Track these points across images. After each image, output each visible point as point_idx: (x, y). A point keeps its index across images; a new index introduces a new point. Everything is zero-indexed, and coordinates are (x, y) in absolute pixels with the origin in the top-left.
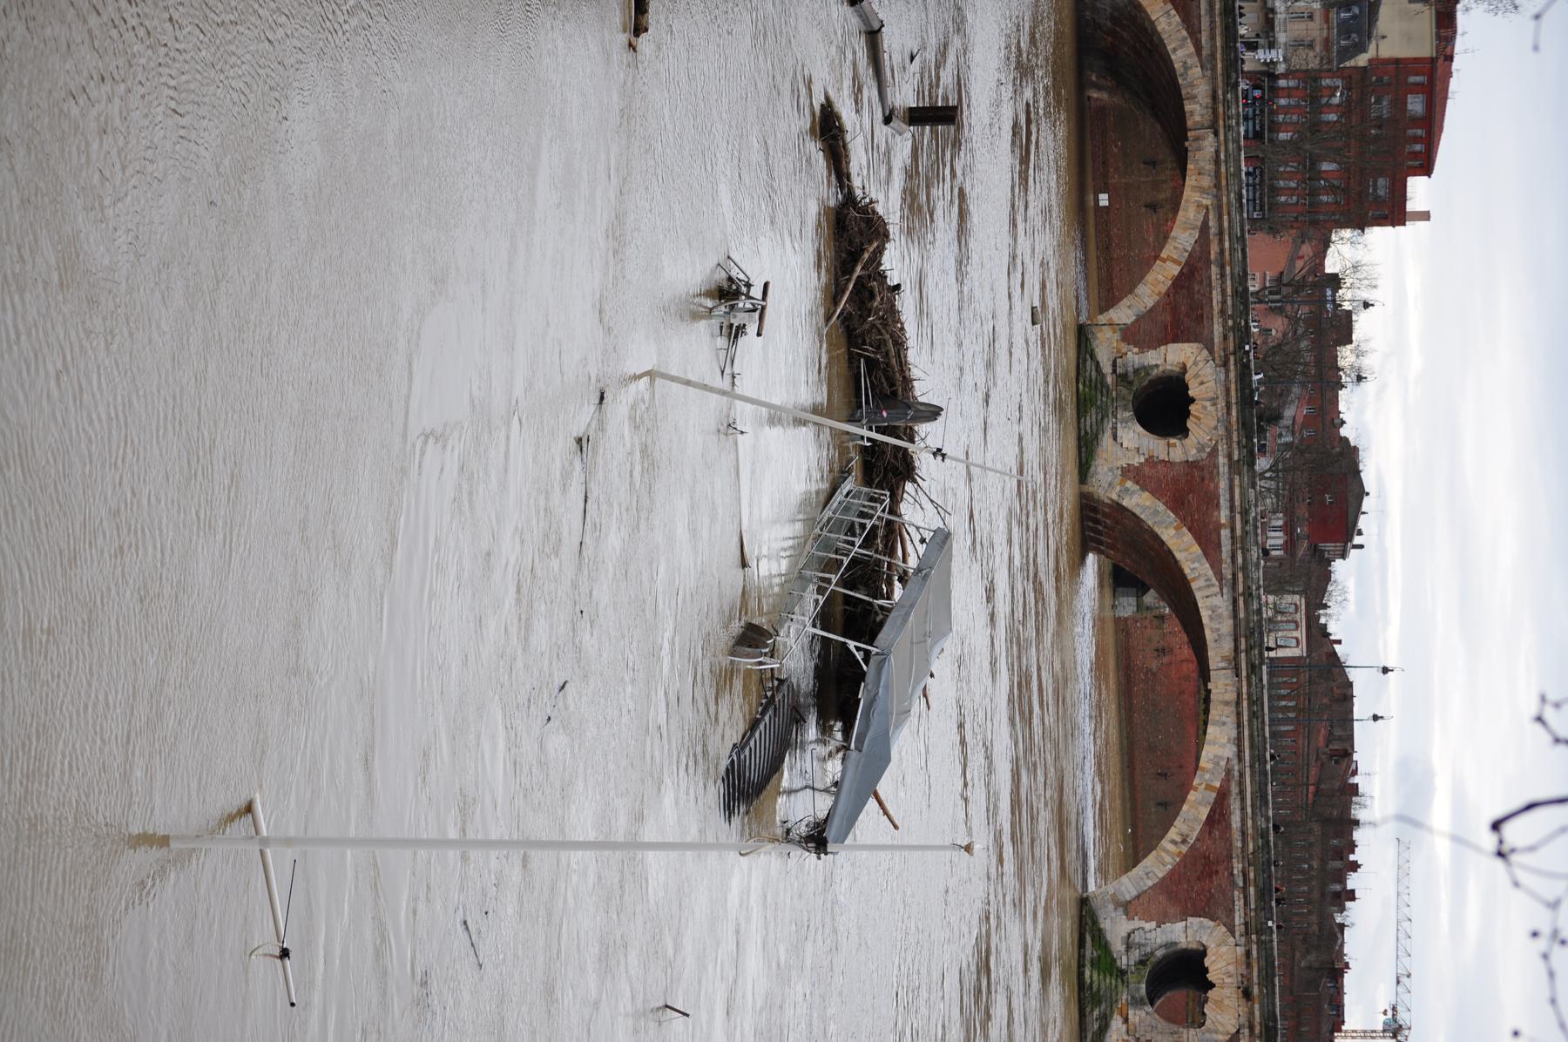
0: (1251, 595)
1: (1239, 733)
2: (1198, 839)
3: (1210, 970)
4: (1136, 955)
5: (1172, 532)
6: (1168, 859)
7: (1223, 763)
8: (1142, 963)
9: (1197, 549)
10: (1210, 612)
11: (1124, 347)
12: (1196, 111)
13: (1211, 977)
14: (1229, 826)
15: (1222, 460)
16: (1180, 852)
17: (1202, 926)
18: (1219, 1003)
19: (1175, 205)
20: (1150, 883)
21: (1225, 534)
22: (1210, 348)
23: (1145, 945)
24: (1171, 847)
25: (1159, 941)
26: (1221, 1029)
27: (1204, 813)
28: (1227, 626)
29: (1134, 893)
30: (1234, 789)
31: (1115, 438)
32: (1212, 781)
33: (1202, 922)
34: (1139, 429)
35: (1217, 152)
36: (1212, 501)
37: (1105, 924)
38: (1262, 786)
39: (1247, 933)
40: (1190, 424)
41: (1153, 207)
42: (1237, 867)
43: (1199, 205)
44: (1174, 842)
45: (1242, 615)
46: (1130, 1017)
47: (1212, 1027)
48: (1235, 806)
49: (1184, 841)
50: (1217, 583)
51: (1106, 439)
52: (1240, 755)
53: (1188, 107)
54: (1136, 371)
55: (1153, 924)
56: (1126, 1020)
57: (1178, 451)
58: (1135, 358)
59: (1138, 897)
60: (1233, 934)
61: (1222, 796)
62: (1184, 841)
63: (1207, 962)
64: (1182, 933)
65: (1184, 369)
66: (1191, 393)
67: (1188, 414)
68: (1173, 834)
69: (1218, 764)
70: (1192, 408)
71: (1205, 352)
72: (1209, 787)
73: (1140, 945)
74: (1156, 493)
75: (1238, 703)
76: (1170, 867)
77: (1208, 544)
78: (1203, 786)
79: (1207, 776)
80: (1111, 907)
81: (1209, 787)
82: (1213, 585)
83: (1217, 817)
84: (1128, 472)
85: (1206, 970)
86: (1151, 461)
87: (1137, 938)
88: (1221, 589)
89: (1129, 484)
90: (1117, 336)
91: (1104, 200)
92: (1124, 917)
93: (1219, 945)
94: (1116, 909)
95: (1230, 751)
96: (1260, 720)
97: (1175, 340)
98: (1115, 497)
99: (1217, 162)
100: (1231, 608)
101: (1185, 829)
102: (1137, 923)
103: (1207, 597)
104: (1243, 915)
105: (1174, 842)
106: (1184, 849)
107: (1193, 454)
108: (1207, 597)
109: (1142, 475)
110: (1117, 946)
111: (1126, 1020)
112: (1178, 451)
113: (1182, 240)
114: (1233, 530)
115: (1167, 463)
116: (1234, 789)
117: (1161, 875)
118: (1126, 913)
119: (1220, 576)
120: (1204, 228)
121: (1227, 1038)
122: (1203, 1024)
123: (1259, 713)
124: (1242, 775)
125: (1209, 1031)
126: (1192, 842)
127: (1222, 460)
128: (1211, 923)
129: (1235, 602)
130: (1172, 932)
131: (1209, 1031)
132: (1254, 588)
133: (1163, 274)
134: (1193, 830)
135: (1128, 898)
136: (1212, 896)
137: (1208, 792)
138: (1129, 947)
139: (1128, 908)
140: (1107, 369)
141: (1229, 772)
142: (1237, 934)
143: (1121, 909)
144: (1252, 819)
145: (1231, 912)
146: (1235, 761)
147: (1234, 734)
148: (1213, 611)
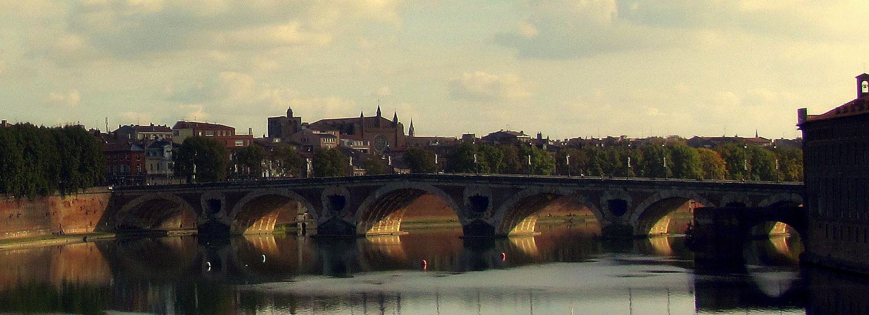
15: (226, 191)
42: (311, 187)
56: (344, 217)
57: (223, 202)
61: (295, 191)
66: (211, 199)
75: (276, 187)
139: (320, 215)
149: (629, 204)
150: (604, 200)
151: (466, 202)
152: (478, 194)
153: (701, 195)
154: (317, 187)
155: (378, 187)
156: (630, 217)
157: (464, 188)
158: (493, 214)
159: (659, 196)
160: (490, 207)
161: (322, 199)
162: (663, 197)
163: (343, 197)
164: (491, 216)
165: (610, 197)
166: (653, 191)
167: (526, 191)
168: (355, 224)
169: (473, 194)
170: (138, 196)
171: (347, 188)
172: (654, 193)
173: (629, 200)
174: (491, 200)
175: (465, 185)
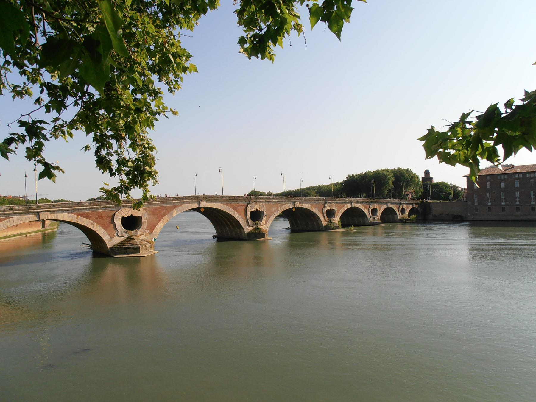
0: (12, 209)
1: (60, 211)
2: (92, 220)
3: (128, 215)
4: (125, 234)
6: (98, 228)
7: (69, 215)
8: (126, 233)
10: (19, 221)
16: (96, 225)
17: (116, 218)
18: (136, 213)
20: (105, 232)
23: (122, 232)
24: (95, 227)
25: (121, 229)
26: (142, 212)
27: (84, 219)
28: (24, 217)
29: (108, 235)
32: (75, 218)
33: (116, 218)
37: (117, 242)
38: (76, 204)
44: (93, 227)
45: (21, 211)
46: (140, 234)
47: (142, 214)
49: (93, 224)
50: (8, 219)
59: (109, 235)
61: (79, 215)
62: (93, 224)
69: (70, 216)
73: (122, 233)
76: (100, 227)
78: (77, 220)
79: (74, 219)
81: (77, 218)
82: (9, 220)
85: (128, 216)
88: (10, 218)
92: (114, 238)
94: (112, 240)
95: (66, 214)
96: (56, 205)
100: (17, 215)
101: (90, 224)
103: (14, 222)
104: (113, 208)
105: (93, 227)
106: (95, 224)
108: (14, 222)
110: (122, 239)
111: (141, 235)
117: (103, 229)
118: (114, 237)
121: (144, 211)
122: (141, 217)
123: (54, 205)
124: (73, 210)
125: (143, 215)
126: (93, 222)
128: (116, 216)
129: (15, 214)
130: (118, 226)
131: (143, 215)
132: (10, 208)
134: (89, 222)
135: (109, 237)
136: (108, 216)
137: (78, 218)
139: (112, 238)
142: (118, 209)
143: (112, 239)
144: (87, 206)
146: (69, 211)
148: (19, 220)
149: (336, 212)
152: (257, 209)
155: (175, 207)
158: (266, 222)
160: (264, 219)
162: (349, 207)
163: (140, 218)
165: (328, 208)
167: (285, 206)
168: (154, 241)
169: (253, 210)
173: (336, 210)
174: (265, 213)
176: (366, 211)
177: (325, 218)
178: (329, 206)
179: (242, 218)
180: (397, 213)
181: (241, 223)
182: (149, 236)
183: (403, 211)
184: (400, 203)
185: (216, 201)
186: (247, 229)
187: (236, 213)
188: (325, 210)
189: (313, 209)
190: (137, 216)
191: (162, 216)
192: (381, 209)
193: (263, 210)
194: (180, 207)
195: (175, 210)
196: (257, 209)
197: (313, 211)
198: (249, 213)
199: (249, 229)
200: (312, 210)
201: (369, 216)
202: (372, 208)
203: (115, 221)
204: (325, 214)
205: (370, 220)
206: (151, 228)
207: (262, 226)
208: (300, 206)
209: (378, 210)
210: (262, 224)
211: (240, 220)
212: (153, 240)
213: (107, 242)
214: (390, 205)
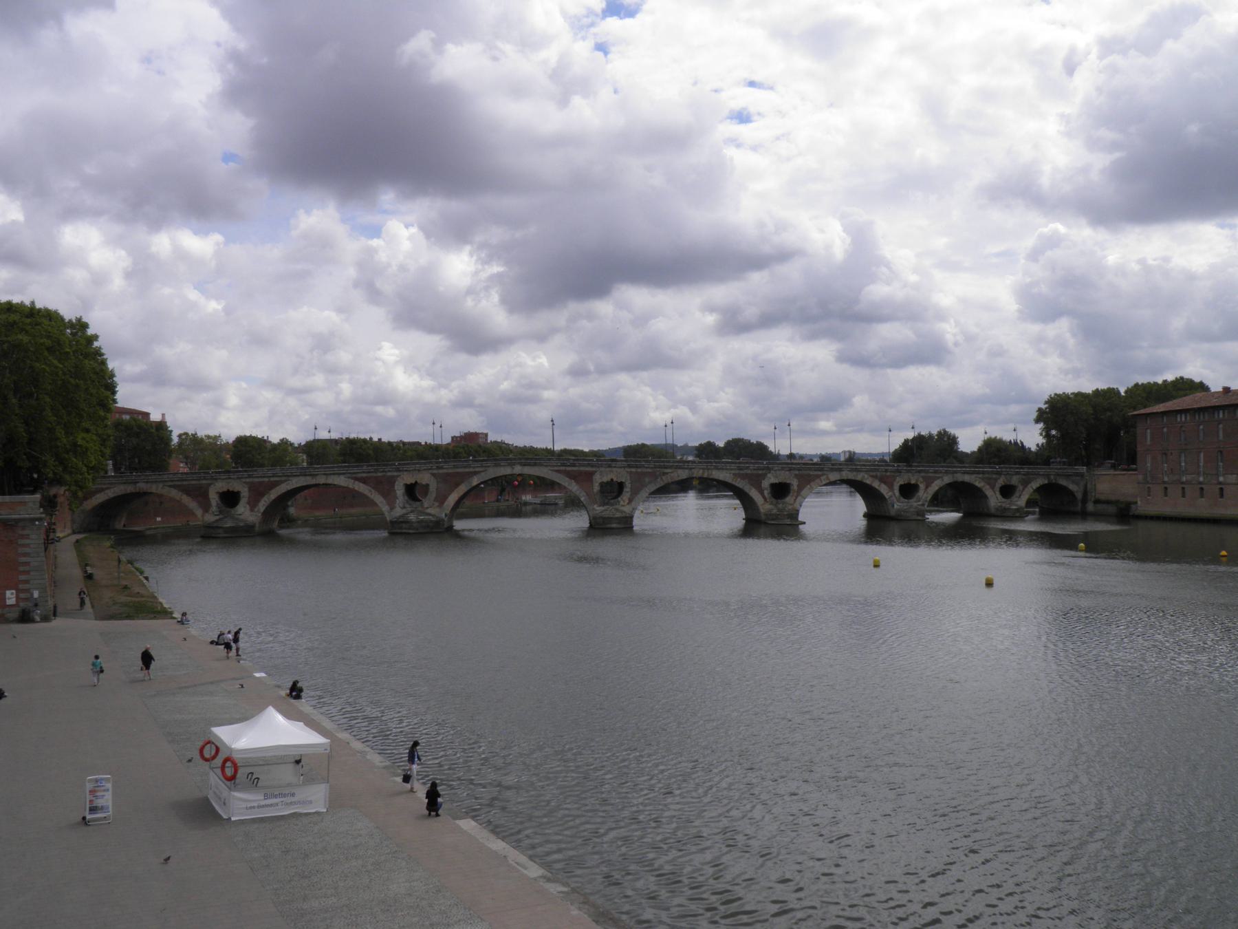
2: (370, 486)
4: (407, 506)
5: (271, 496)
7: (347, 479)
9: (278, 488)
11: (210, 512)
12: (130, 489)
13: (413, 482)
14: (366, 477)
15: (248, 480)
19: (160, 496)
21: (272, 479)
22: (210, 485)
27: (361, 484)
28: (302, 478)
30: (354, 475)
31: (240, 515)
34: (238, 506)
35: (144, 482)
36: (261, 483)
37: (398, 515)
39: (400, 471)
40: (236, 490)
41: (161, 503)
43: (162, 488)
48: (360, 475)
49: (371, 491)
51: (241, 517)
52: (344, 474)
53: (129, 492)
54: (219, 508)
55: (397, 500)
56: (427, 508)
57: (245, 493)
58: (214, 508)
60: (400, 475)
61: (356, 479)
63: (408, 483)
64: (400, 491)
65: (218, 493)
67: (233, 492)
68: (369, 495)
70: (231, 490)
71: (212, 486)
72: (354, 483)
74: (258, 501)
77: (274, 485)
80: (392, 513)
81: (354, 483)
83: (364, 481)
84: (252, 510)
86: (249, 503)
87: (401, 505)
89: (256, 510)
90: (207, 514)
91: (159, 519)
93: (403, 479)
95: (342, 477)
97: (208, 495)
98: (260, 514)
99: (147, 482)
102: (397, 505)
106: (373, 491)
107: (246, 489)
109: (253, 504)
110: (404, 511)
111: (427, 508)
112: (245, 493)
113: (174, 493)
114: (270, 477)
115: (249, 498)
116: (354, 475)
119: (286, 481)
120: (170, 486)
121: (432, 477)
127: (248, 480)
133: (186, 500)
138: (404, 507)
139: (392, 508)
140: (217, 517)
141: (349, 478)
145: (393, 477)
147: (337, 476)
149: (795, 488)
150: (766, 484)
151: (596, 488)
152: (612, 480)
153: (872, 476)
154: (389, 474)
155: (475, 473)
156: (795, 500)
157: (596, 472)
158: (630, 501)
159: (828, 478)
161: (396, 487)
163: (427, 485)
164: (628, 504)
165: (774, 480)
166: (820, 473)
167: (672, 475)
169: (606, 479)
170: (108, 488)
171: (433, 475)
172: (823, 475)
173: (795, 484)
175: (594, 469)
176: (884, 489)
177: (765, 499)
178: (776, 477)
179: (585, 492)
180: (988, 492)
181: (582, 499)
182: (438, 510)
183: (1007, 491)
184: (999, 474)
185: (542, 465)
186: (594, 509)
187: (574, 484)
188: (766, 484)
189: (736, 481)
190: (424, 483)
191: (457, 485)
192: (933, 485)
193: (623, 481)
194: (483, 474)
195: (475, 477)
196: (612, 480)
197: (737, 485)
198: (597, 484)
199: (596, 510)
200: (734, 483)
201: (894, 498)
202: (902, 483)
203: (396, 488)
204: (766, 493)
205: (896, 506)
206: (441, 500)
207: (623, 506)
208: (705, 476)
209: (922, 486)
210: (622, 503)
211: (581, 495)
212: (444, 515)
213: (386, 514)
214: (961, 478)
